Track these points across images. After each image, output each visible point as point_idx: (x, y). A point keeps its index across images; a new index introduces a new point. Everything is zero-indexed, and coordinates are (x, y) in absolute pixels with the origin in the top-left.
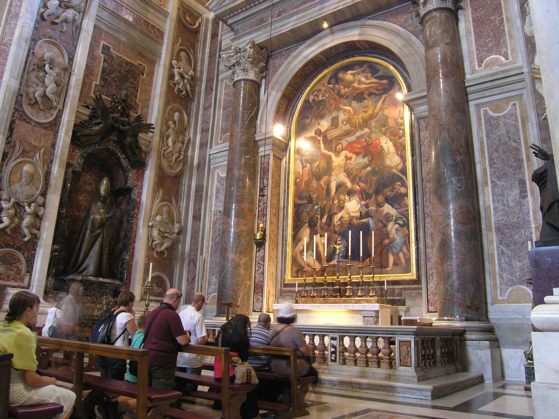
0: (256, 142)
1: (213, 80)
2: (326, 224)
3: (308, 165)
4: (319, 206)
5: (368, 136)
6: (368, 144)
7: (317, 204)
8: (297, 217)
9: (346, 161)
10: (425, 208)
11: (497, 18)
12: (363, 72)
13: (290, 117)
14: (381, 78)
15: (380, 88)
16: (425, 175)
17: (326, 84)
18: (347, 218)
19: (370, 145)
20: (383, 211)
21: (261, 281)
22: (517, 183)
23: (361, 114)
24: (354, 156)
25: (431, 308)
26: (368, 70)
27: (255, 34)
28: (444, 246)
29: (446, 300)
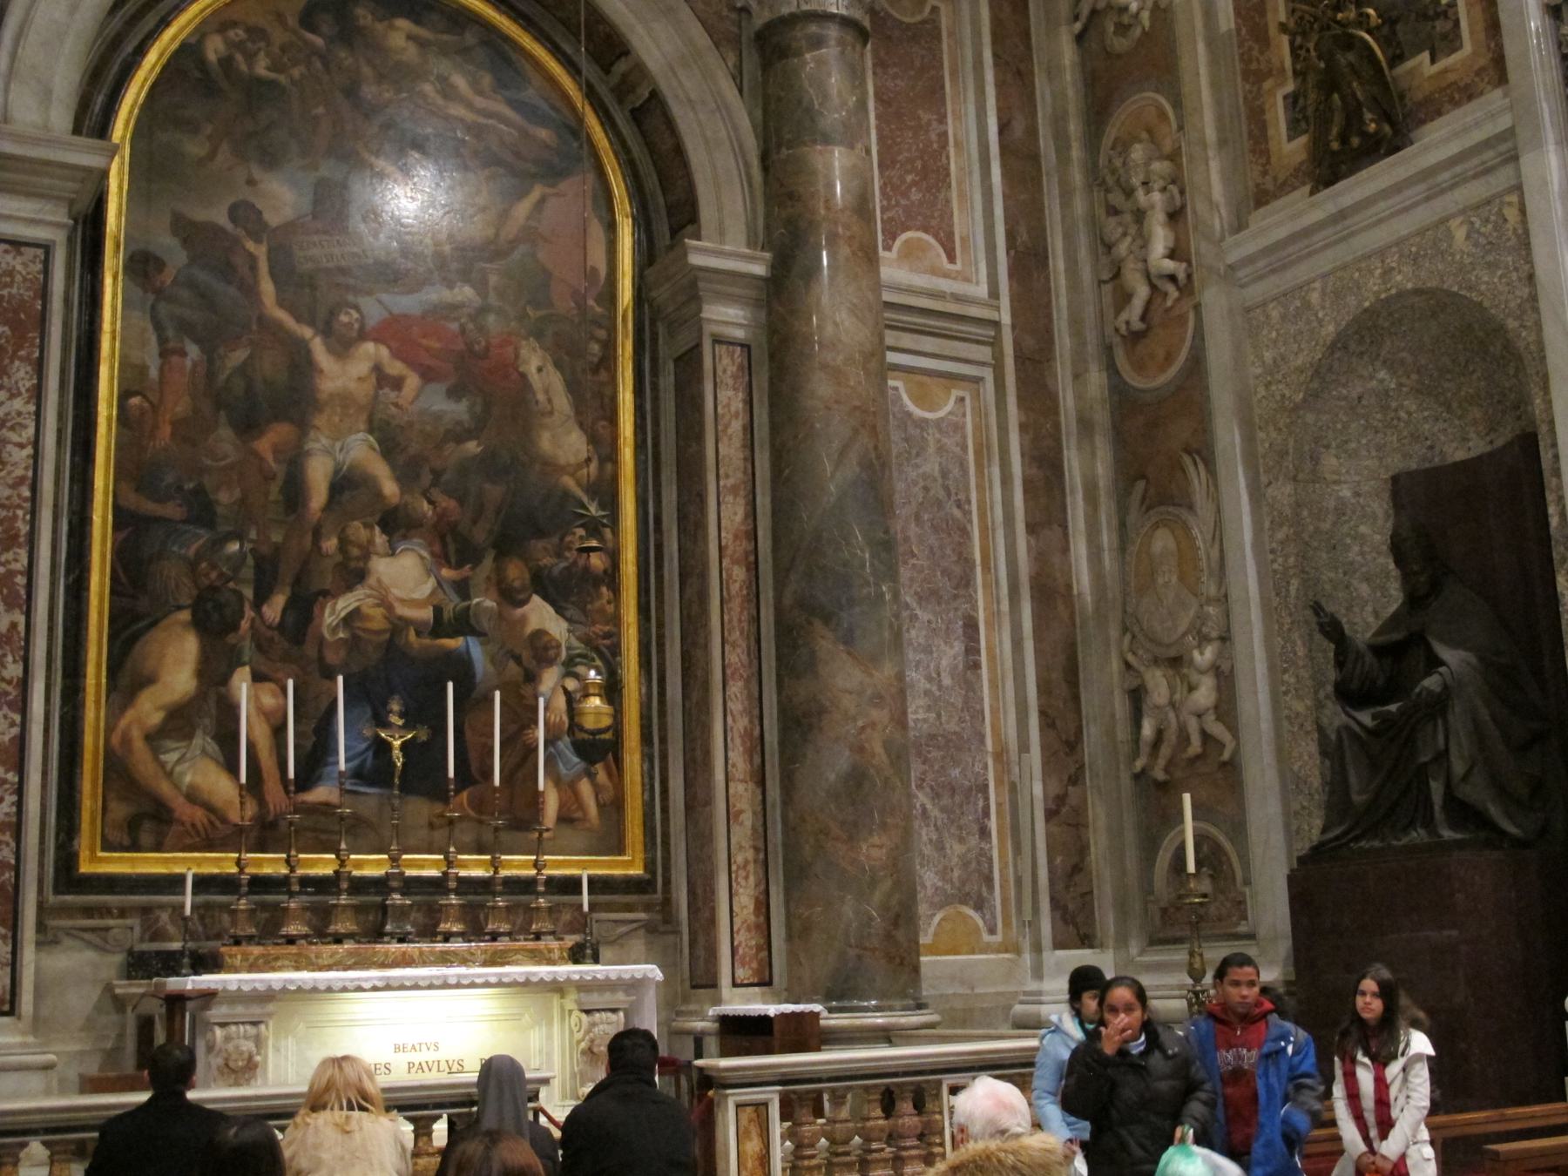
2: (281, 627)
3: (193, 351)
4: (248, 546)
5: (472, 318)
7: (239, 536)
9: (380, 386)
10: (727, 648)
11: (935, 124)
12: (464, 51)
16: (730, 536)
17: (292, 21)
18: (377, 619)
20: (523, 620)
22: (961, 623)
24: (413, 381)
25: (741, 974)
28: (859, 785)
29: (865, 949)
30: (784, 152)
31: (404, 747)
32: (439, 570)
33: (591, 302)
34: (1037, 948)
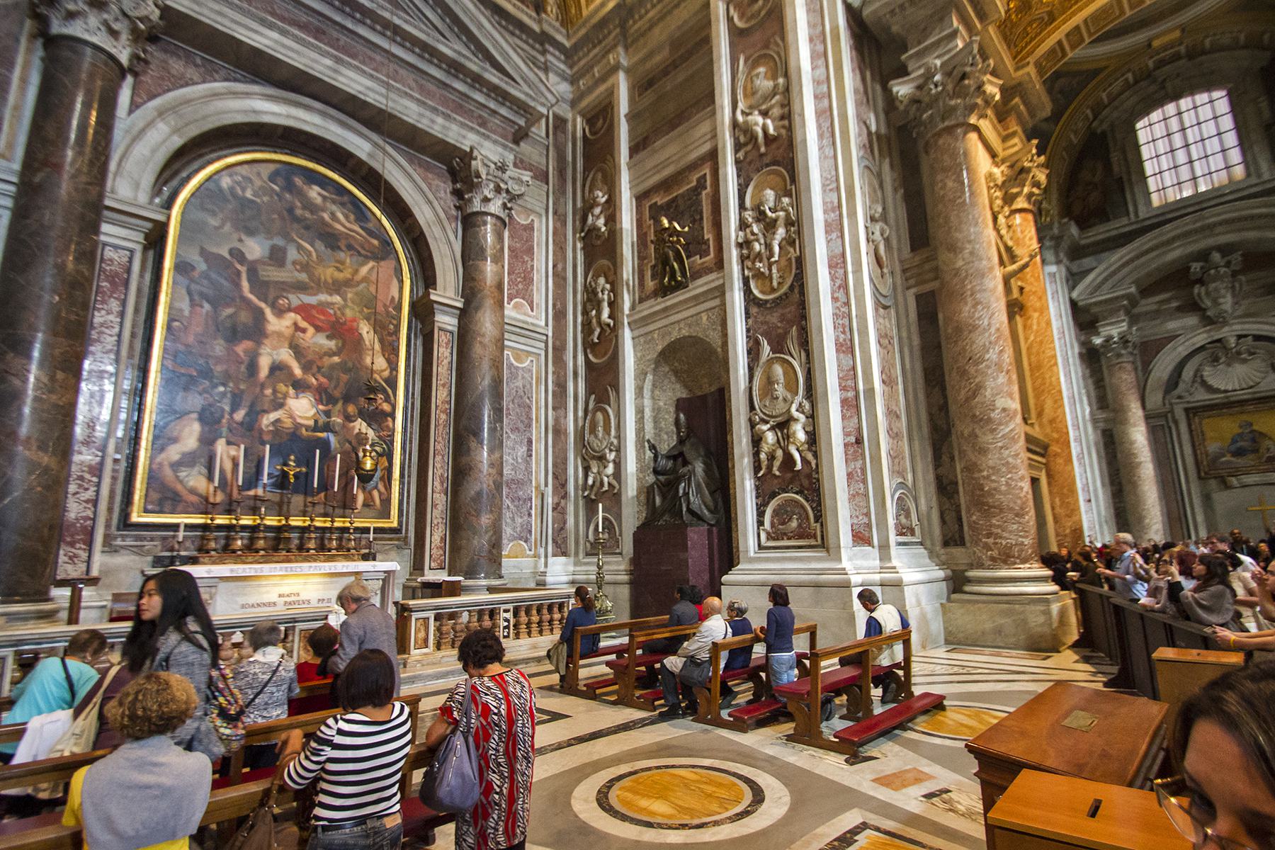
2: (241, 424)
3: (207, 306)
4: (229, 389)
5: (339, 309)
6: (337, 321)
7: (224, 385)
12: (343, 204)
14: (370, 233)
15: (366, 246)
17: (265, 178)
19: (341, 324)
20: (354, 427)
24: (311, 330)
26: (349, 206)
30: (471, 262)
31: (295, 476)
33: (391, 309)
34: (546, 556)
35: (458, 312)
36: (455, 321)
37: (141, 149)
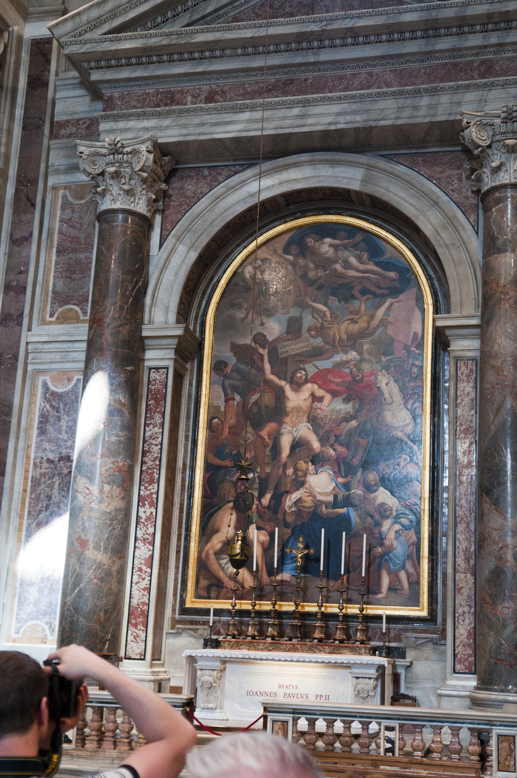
0: (143, 339)
1: (35, 182)
2: (268, 508)
3: (238, 398)
4: (256, 475)
5: (355, 365)
6: (354, 378)
7: (253, 471)
8: (209, 487)
10: (458, 508)
12: (355, 246)
13: (202, 297)
14: (387, 266)
17: (280, 252)
19: (357, 382)
21: (144, 604)
23: (346, 323)
24: (328, 397)
26: (362, 245)
27: (155, 121)
29: (498, 660)
32: (337, 479)
33: (413, 349)
35: (477, 331)
36: (476, 344)
37: (168, 276)
